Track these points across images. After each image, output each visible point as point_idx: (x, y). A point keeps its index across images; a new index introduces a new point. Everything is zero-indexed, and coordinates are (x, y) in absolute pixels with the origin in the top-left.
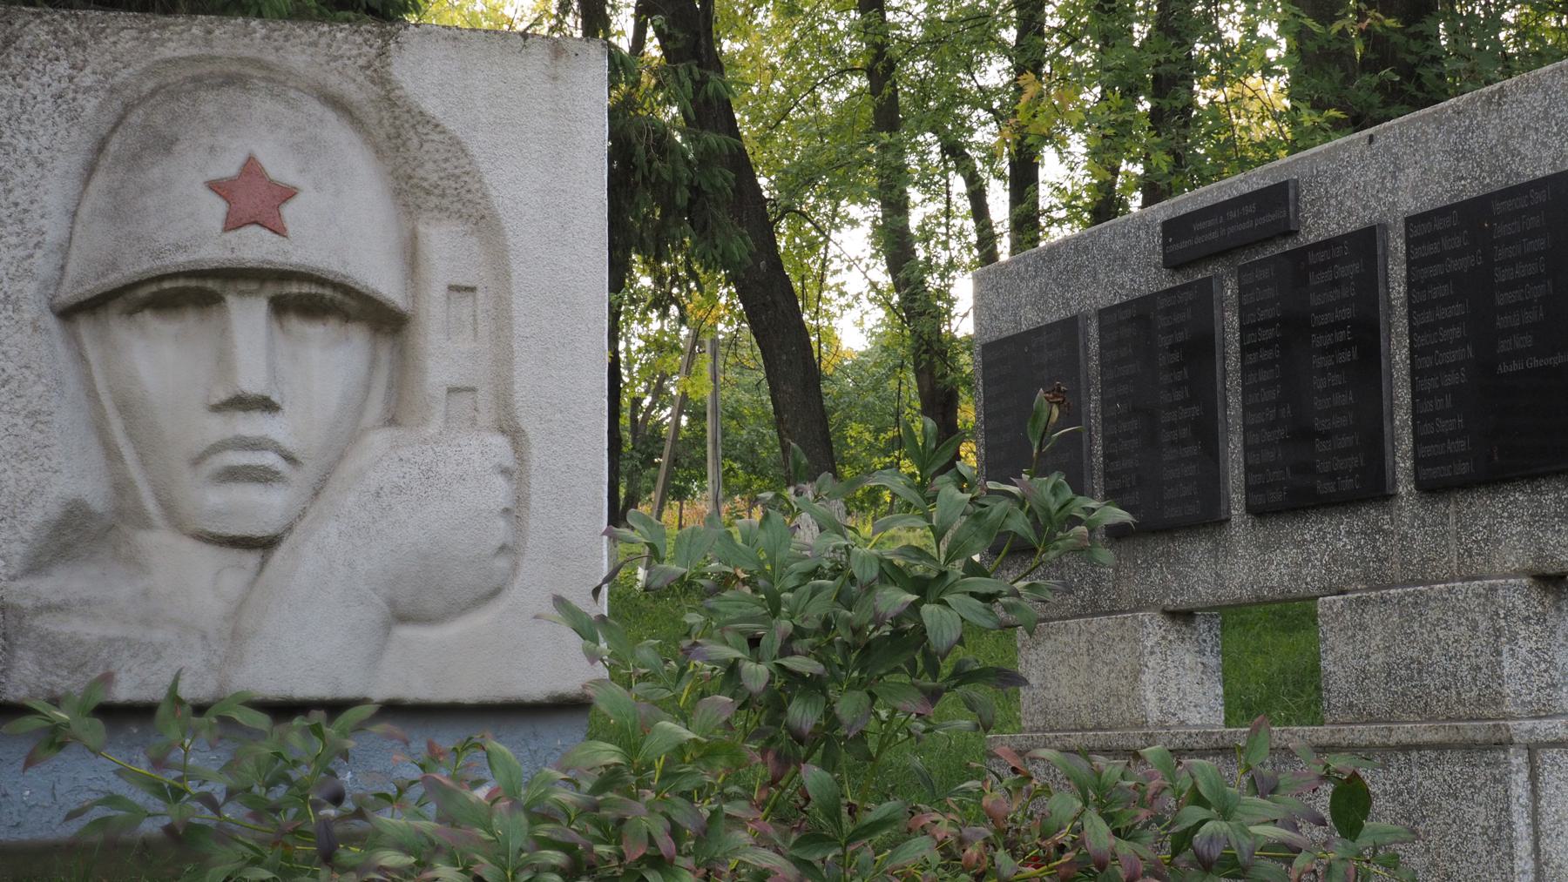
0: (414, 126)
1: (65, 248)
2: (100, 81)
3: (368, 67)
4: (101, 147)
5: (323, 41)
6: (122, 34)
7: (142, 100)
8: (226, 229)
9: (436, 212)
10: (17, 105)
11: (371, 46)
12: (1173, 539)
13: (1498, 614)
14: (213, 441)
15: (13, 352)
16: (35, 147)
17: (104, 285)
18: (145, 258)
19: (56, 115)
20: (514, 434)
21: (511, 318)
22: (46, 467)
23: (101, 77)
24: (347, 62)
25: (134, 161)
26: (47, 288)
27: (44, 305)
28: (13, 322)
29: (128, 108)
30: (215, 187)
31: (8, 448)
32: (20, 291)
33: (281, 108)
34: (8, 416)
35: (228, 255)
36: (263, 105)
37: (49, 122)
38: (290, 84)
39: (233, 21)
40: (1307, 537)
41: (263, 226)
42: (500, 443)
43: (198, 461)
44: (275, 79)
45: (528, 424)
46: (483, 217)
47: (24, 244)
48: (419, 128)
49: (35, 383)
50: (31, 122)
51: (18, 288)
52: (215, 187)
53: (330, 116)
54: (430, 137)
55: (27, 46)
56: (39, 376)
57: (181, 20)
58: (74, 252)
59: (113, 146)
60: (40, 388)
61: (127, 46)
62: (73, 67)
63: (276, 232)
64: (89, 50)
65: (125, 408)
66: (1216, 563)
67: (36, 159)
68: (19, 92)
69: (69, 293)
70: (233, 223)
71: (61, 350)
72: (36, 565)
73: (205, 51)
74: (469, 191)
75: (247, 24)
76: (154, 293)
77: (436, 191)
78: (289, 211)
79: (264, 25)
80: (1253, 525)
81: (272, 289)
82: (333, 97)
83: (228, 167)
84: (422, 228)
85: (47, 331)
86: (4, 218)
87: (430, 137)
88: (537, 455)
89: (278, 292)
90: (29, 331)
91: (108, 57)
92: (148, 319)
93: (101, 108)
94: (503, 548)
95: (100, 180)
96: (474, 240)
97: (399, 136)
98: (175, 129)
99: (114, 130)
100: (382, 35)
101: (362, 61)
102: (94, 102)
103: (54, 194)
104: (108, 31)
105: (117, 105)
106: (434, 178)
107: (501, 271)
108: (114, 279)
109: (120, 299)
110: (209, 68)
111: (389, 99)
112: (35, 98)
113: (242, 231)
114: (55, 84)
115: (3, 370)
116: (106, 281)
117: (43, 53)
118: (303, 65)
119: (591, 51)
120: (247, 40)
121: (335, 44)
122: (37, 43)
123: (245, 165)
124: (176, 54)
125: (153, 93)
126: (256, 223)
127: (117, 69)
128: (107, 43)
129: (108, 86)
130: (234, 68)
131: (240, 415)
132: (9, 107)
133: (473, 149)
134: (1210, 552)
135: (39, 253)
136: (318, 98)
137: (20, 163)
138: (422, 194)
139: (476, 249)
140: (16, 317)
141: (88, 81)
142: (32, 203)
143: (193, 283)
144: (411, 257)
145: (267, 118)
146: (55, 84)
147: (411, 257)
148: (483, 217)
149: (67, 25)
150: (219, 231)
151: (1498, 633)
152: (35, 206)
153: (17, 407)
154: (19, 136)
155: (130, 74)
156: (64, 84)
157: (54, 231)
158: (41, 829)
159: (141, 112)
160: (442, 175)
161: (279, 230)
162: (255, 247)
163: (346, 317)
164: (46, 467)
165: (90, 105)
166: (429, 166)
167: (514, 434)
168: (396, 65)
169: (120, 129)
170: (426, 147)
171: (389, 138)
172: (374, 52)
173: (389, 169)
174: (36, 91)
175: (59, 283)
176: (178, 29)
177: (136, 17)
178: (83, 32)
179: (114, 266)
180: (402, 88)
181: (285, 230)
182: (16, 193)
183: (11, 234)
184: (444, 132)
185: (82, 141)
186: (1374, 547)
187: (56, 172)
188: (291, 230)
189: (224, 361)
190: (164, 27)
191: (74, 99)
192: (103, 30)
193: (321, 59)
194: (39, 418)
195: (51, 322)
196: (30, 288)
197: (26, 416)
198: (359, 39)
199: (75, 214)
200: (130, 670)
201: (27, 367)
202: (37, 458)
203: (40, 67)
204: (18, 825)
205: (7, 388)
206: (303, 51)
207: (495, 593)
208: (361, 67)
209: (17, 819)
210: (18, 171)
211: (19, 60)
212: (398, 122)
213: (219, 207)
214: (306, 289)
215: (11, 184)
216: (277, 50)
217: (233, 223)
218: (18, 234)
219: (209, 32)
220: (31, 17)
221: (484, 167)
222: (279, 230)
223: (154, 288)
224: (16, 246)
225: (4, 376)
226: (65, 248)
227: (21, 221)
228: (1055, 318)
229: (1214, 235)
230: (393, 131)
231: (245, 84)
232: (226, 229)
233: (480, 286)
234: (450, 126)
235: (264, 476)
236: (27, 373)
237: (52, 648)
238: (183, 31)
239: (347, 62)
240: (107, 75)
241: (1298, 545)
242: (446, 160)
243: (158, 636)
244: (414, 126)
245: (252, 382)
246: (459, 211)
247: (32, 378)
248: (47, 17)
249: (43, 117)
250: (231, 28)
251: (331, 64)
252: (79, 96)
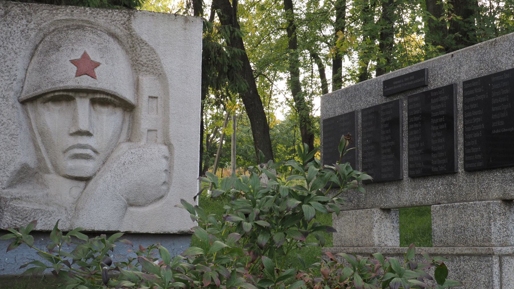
0: (138, 44)
1: (23, 81)
2: (36, 27)
3: (124, 24)
4: (36, 48)
5: (110, 15)
6: (44, 11)
7: (50, 33)
8: (76, 76)
9: (145, 72)
10: (9, 33)
11: (125, 17)
12: (384, 185)
13: (490, 212)
14: (70, 145)
15: (6, 114)
16: (14, 48)
17: (36, 93)
18: (49, 85)
19: (21, 37)
20: (169, 145)
21: (169, 107)
22: (15, 152)
23: (37, 25)
24: (117, 22)
25: (47, 53)
26: (17, 94)
27: (16, 100)
28: (6, 105)
29: (45, 35)
30: (73, 62)
31: (3, 146)
32: (8, 94)
33: (95, 37)
34: (3, 136)
35: (77, 84)
36: (90, 36)
37: (19, 40)
38: (98, 29)
39: (80, 8)
40: (428, 185)
41: (88, 75)
42: (164, 148)
43: (65, 152)
44: (94, 27)
45: (174, 142)
46: (161, 74)
47: (11, 80)
48: (141, 44)
49: (12, 125)
50: (13, 39)
51: (8, 93)
52: (73, 62)
53: (111, 40)
54: (144, 47)
55: (12, 14)
56: (14, 123)
57: (63, 7)
58: (26, 82)
59: (40, 48)
60: (14, 127)
61: (45, 15)
62: (28, 22)
63: (92, 77)
64: (33, 16)
65: (41, 134)
66: (398, 193)
67: (14, 52)
68: (10, 29)
69: (24, 96)
70: (78, 74)
71: (21, 114)
72: (11, 185)
73: (71, 17)
74: (156, 65)
75: (85, 9)
76: (52, 96)
77: (145, 65)
78: (97, 70)
79: (90, 9)
80: (411, 181)
81: (91, 96)
82: (112, 34)
83: (78, 56)
84: (140, 77)
85: (17, 108)
86: (4, 71)
87: (144, 47)
88: (176, 152)
89: (93, 97)
90: (11, 108)
91: (39, 19)
92: (50, 105)
93: (36, 35)
94: (164, 183)
95: (35, 59)
96: (158, 81)
97: (134, 47)
98: (61, 43)
99: (40, 43)
100: (129, 14)
101: (122, 22)
102: (34, 33)
103: (20, 63)
104: (39, 10)
105: (41, 34)
106: (145, 61)
107: (166, 93)
108: (39, 91)
109: (41, 98)
110: (72, 23)
111: (131, 35)
112: (15, 31)
113: (81, 77)
114: (21, 27)
115: (2, 120)
116: (36, 92)
117: (18, 17)
118: (103, 23)
119: (197, 21)
120: (85, 14)
121: (113, 16)
122: (16, 14)
123: (83, 55)
124: (61, 18)
125: (54, 31)
126: (86, 74)
127: (42, 23)
128: (39, 14)
129: (39, 28)
130: (80, 23)
131: (79, 137)
132: (6, 34)
133: (158, 52)
134: (396, 189)
135: (15, 82)
136: (108, 34)
137: (9, 53)
138: (141, 66)
139: (158, 84)
140: (7, 103)
141: (32, 26)
142: (13, 66)
143: (65, 93)
144: (137, 87)
145: (90, 40)
146: (21, 27)
147: (137, 87)
148: (161, 74)
149: (26, 8)
150: (74, 76)
151: (490, 218)
152: (14, 67)
153: (6, 132)
154: (9, 44)
155: (46, 24)
156: (24, 27)
157: (20, 75)
158: (11, 271)
159: (49, 37)
160: (148, 60)
161: (94, 77)
162: (86, 82)
163: (115, 106)
164: (15, 152)
165: (33, 34)
166: (143, 57)
167: (169, 145)
168: (133, 23)
169: (42, 42)
170: (142, 50)
171: (130, 47)
172: (126, 19)
173: (130, 58)
174: (15, 29)
175: (21, 92)
176: (62, 10)
177: (48, 6)
178: (31, 10)
179: (39, 87)
180: (135, 31)
181: (96, 77)
182: (8, 63)
183: (6, 76)
184: (148, 46)
185: (30, 46)
186: (450, 189)
187: (21, 56)
188: (97, 77)
189: (75, 119)
190: (58, 9)
191: (28, 32)
192: (38, 10)
193: (109, 21)
194: (14, 136)
195: (18, 105)
196: (12, 94)
197: (9, 136)
198: (121, 15)
199: (27, 70)
200: (41, 220)
201: (10, 120)
202: (13, 149)
203: (17, 21)
204: (3, 269)
205: (3, 126)
206: (103, 18)
207: (162, 197)
208: (122, 24)
209: (3, 268)
210: (8, 55)
211: (10, 19)
212: (133, 42)
213: (75, 69)
214: (102, 96)
215: (6, 59)
216: (94, 18)
217: (78, 74)
218: (8, 76)
219: (72, 11)
220: (14, 5)
221: (162, 57)
222: (94, 77)
223: (52, 95)
224: (7, 80)
225: (2, 122)
226: (23, 81)
227: (9, 72)
228: (347, 112)
229: (400, 86)
230: (132, 45)
231: (84, 28)
232: (76, 76)
233: (159, 97)
234: (150, 44)
235: (87, 157)
236: (10, 121)
237: (15, 212)
238: (64, 11)
239: (117, 22)
240: (39, 25)
241: (425, 188)
242: (149, 55)
243: (51, 209)
244: (138, 44)
245: (83, 126)
246: (153, 72)
247: (12, 123)
248: (19, 5)
249: (17, 38)
250: (79, 10)
251: (112, 23)
252: (29, 31)
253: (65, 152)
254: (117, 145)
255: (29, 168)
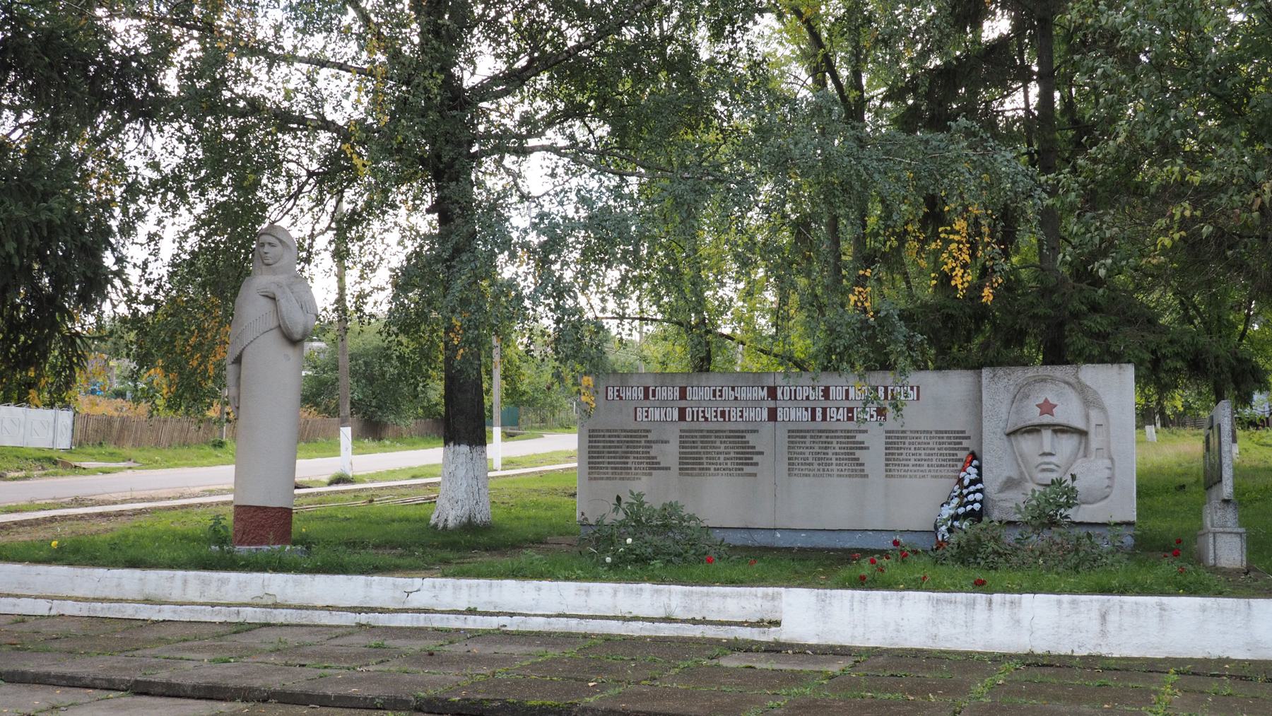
1: (1007, 420)
20: (1111, 459)
42: (1107, 462)
71: (1006, 443)
72: (1001, 491)
83: (1041, 401)
94: (1108, 487)
103: (1004, 409)
144: (1087, 418)
147: (1087, 418)
157: (1004, 417)
161: (1052, 415)
163: (1072, 433)
167: (1111, 459)
207: (1106, 497)
213: (1039, 410)
222: (1052, 415)
226: (1007, 420)
253: (1037, 467)
254: (1074, 461)
255: (1014, 480)
